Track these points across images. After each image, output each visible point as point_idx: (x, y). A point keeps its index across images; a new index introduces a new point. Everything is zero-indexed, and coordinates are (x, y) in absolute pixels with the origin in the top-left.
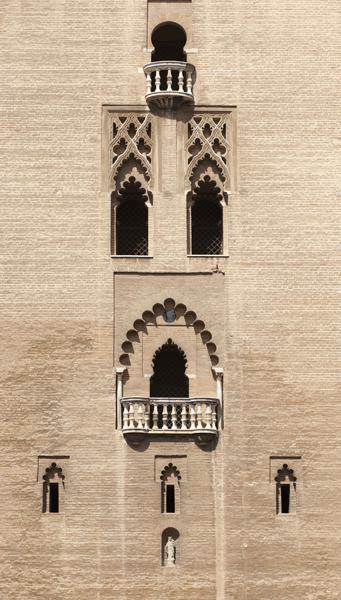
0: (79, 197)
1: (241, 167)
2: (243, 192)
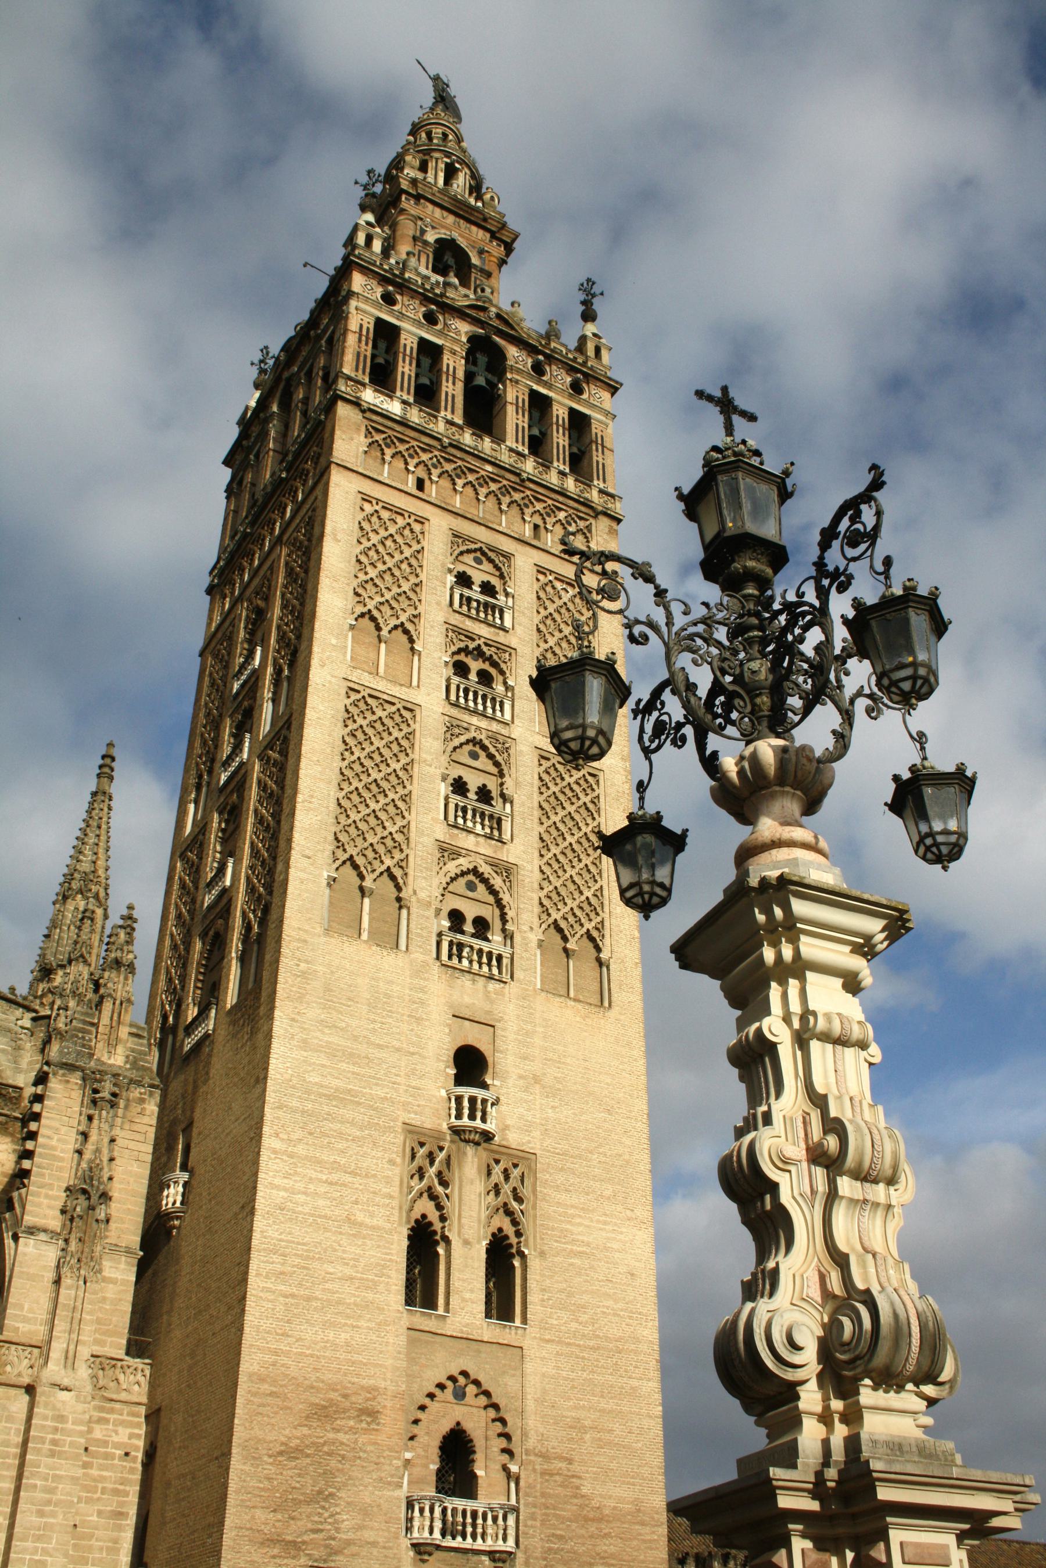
0: (373, 1228)
2: (542, 1254)
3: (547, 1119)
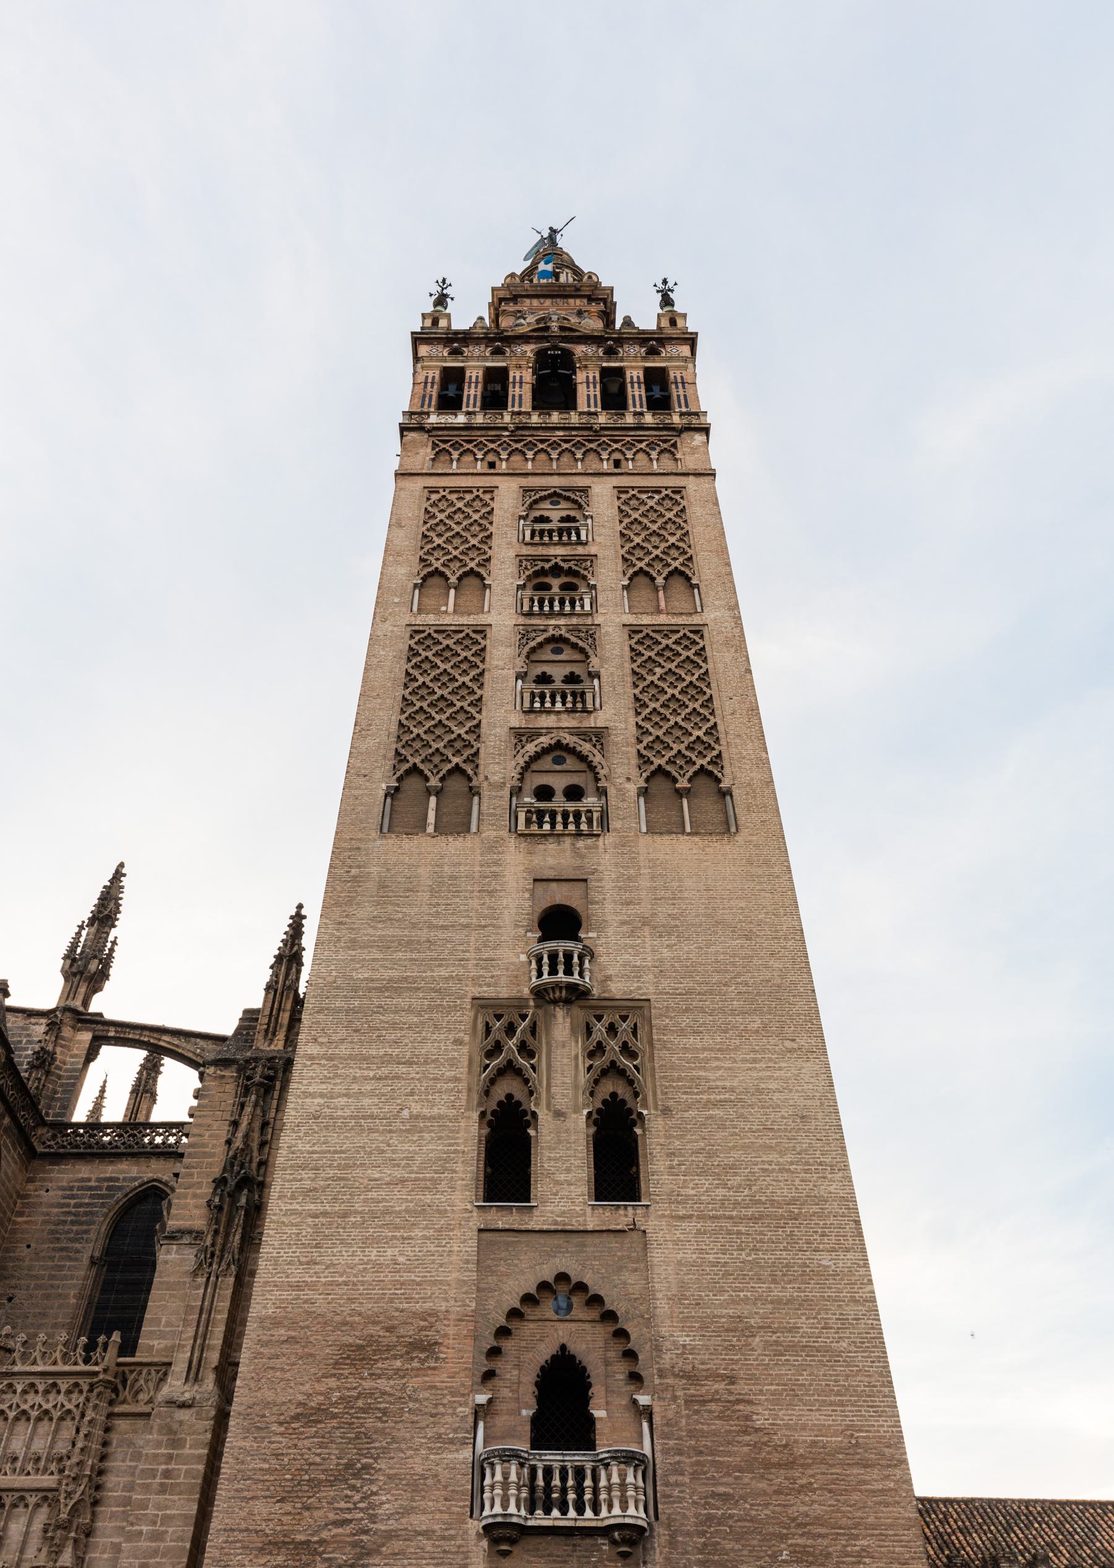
1: (661, 1078)
2: (666, 1111)
3: (661, 961)
